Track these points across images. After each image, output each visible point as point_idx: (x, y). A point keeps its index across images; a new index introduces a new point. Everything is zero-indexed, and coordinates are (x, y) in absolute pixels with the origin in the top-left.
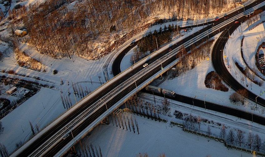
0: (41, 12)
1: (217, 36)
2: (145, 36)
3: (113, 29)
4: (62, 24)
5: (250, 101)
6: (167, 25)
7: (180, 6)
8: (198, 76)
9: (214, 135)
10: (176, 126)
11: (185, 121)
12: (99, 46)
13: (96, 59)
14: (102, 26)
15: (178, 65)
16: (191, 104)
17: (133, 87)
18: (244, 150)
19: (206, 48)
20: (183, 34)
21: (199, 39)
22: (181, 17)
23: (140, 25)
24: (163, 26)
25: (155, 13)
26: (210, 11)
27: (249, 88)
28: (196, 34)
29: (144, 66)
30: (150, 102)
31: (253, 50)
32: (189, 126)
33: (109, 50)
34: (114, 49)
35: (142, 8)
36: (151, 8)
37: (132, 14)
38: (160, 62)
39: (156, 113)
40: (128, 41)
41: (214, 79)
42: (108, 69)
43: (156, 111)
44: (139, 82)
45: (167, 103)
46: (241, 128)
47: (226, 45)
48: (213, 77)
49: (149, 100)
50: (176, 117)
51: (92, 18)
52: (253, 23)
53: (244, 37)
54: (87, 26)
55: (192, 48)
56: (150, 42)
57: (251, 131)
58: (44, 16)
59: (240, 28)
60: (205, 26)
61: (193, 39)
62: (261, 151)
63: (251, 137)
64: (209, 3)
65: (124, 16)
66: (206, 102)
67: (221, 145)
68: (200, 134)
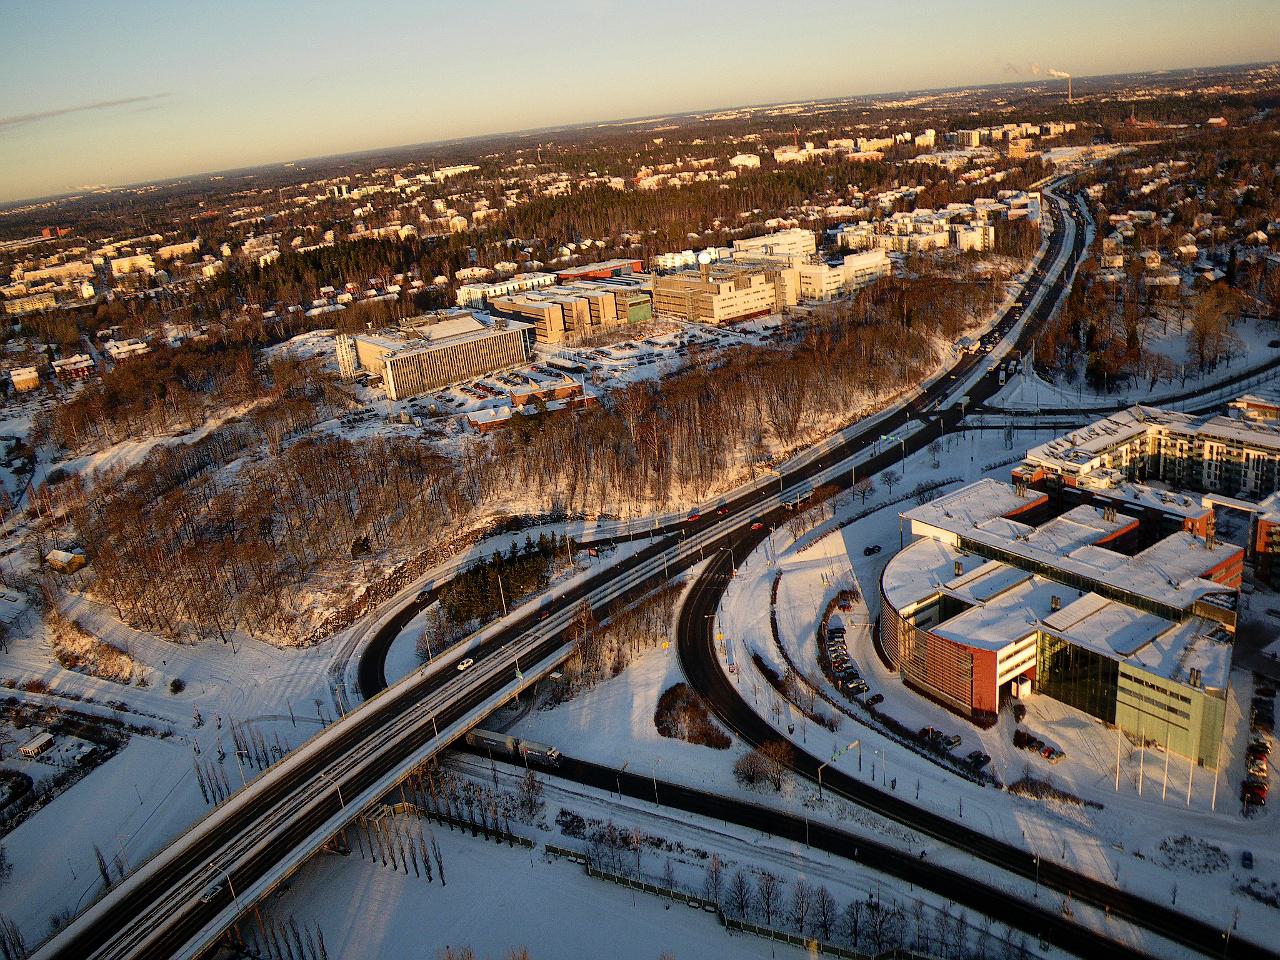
0: (132, 493)
1: (696, 571)
2: (464, 571)
3: (362, 547)
4: (199, 533)
5: (801, 780)
6: (534, 534)
7: (576, 473)
8: (635, 698)
9: (684, 887)
10: (563, 859)
11: (591, 845)
12: (316, 603)
13: (306, 644)
14: (326, 538)
15: (570, 664)
16: (612, 789)
17: (426, 734)
18: (780, 937)
19: (661, 610)
20: (586, 565)
21: (637, 582)
22: (579, 510)
23: (447, 535)
24: (520, 539)
25: (495, 498)
26: (673, 490)
27: (796, 739)
28: (628, 564)
29: (461, 667)
30: (480, 781)
31: (810, 616)
32: (605, 860)
33: (349, 616)
34: (366, 612)
35: (455, 481)
36: (482, 481)
37: (423, 500)
38: (513, 653)
39: (501, 819)
40: (408, 587)
41: (685, 710)
42: (345, 676)
43: (500, 811)
44: (446, 719)
45: (533, 786)
46: (771, 867)
47: (724, 600)
48: (680, 704)
49: (477, 774)
50: (563, 832)
51: (295, 512)
52: (809, 528)
53: (780, 573)
54: (278, 541)
55: (614, 609)
56: (480, 590)
57: (802, 876)
58: (141, 506)
59: (768, 545)
60: (657, 539)
61: (617, 579)
62: (835, 941)
63: (802, 893)
64: (668, 465)
65: (397, 507)
66: (660, 784)
67: (708, 921)
68: (638, 885)
